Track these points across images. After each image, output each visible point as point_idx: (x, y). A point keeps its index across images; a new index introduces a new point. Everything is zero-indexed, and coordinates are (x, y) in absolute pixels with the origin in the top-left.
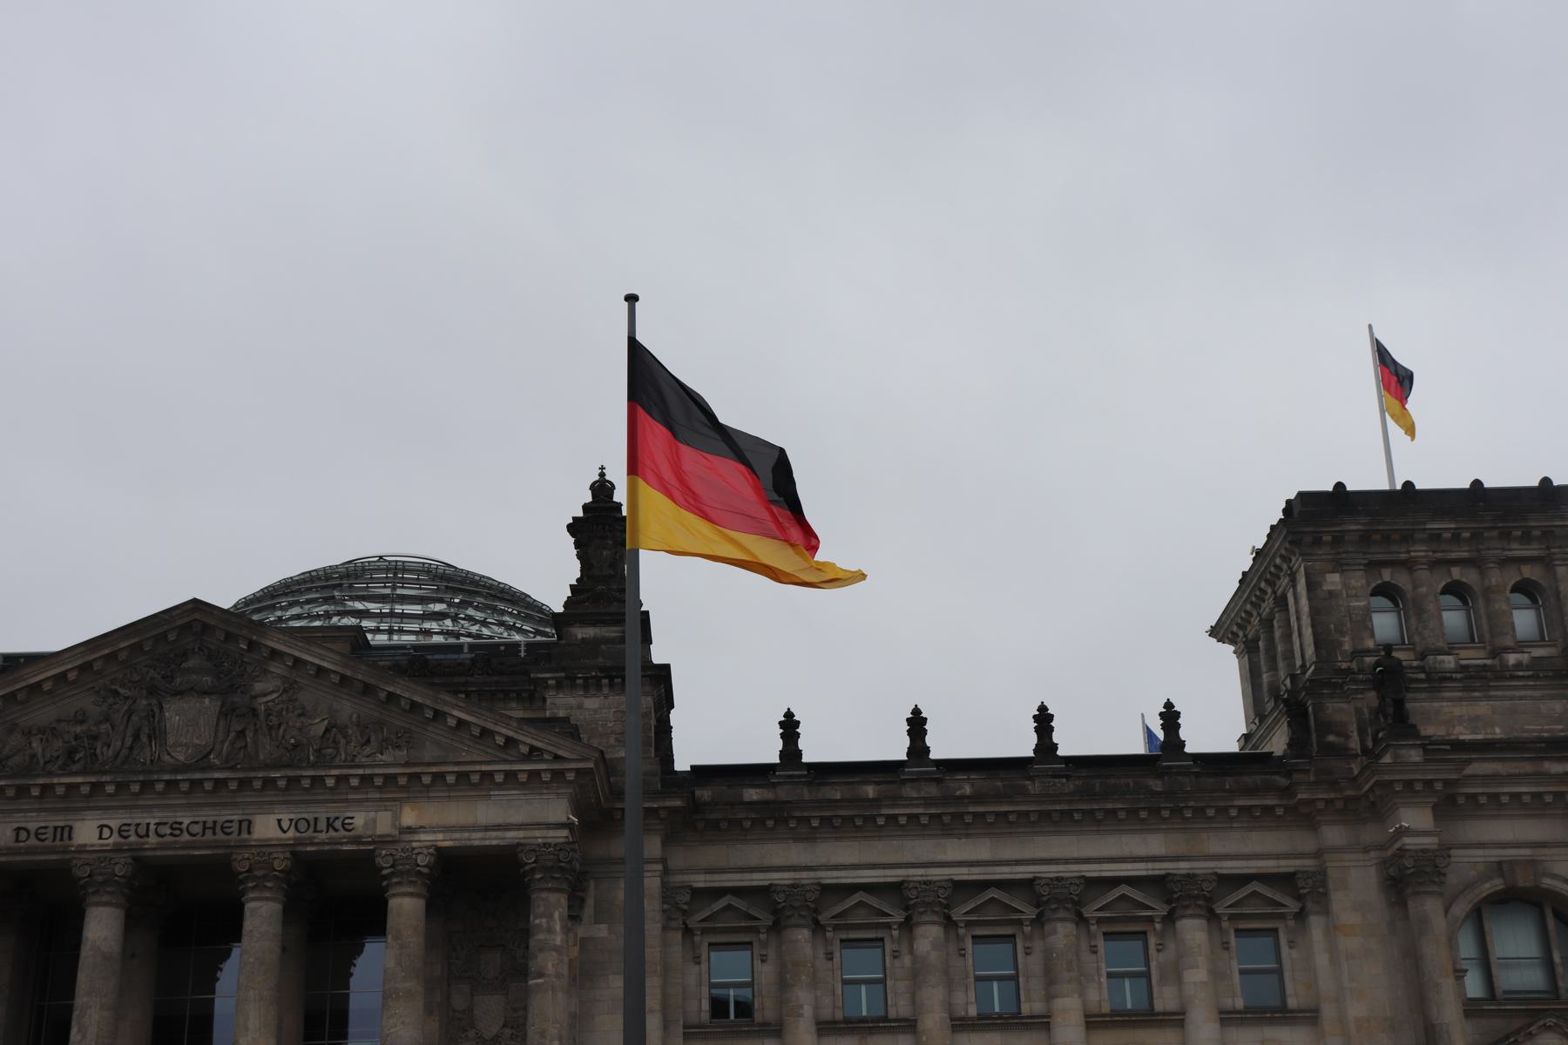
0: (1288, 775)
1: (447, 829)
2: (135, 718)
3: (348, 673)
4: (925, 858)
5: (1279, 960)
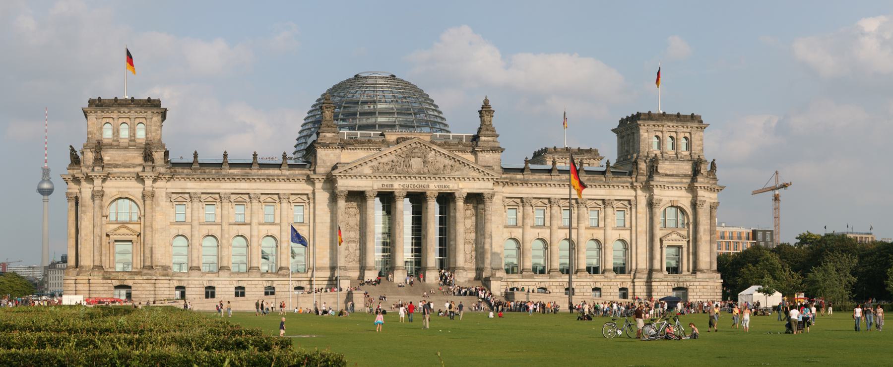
0: (632, 178)
1: (469, 189)
2: (406, 162)
3: (450, 155)
4: (556, 193)
5: (625, 217)
